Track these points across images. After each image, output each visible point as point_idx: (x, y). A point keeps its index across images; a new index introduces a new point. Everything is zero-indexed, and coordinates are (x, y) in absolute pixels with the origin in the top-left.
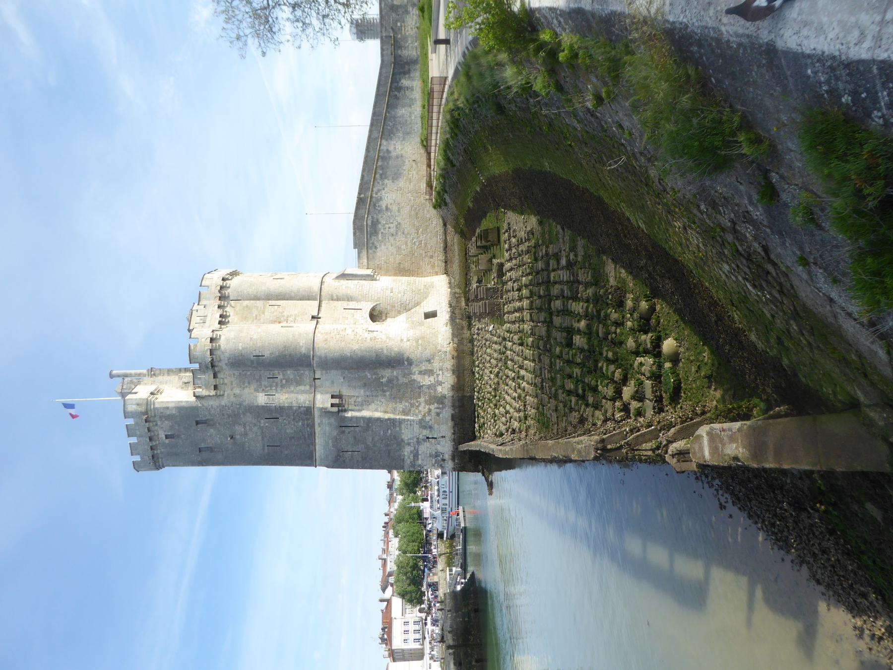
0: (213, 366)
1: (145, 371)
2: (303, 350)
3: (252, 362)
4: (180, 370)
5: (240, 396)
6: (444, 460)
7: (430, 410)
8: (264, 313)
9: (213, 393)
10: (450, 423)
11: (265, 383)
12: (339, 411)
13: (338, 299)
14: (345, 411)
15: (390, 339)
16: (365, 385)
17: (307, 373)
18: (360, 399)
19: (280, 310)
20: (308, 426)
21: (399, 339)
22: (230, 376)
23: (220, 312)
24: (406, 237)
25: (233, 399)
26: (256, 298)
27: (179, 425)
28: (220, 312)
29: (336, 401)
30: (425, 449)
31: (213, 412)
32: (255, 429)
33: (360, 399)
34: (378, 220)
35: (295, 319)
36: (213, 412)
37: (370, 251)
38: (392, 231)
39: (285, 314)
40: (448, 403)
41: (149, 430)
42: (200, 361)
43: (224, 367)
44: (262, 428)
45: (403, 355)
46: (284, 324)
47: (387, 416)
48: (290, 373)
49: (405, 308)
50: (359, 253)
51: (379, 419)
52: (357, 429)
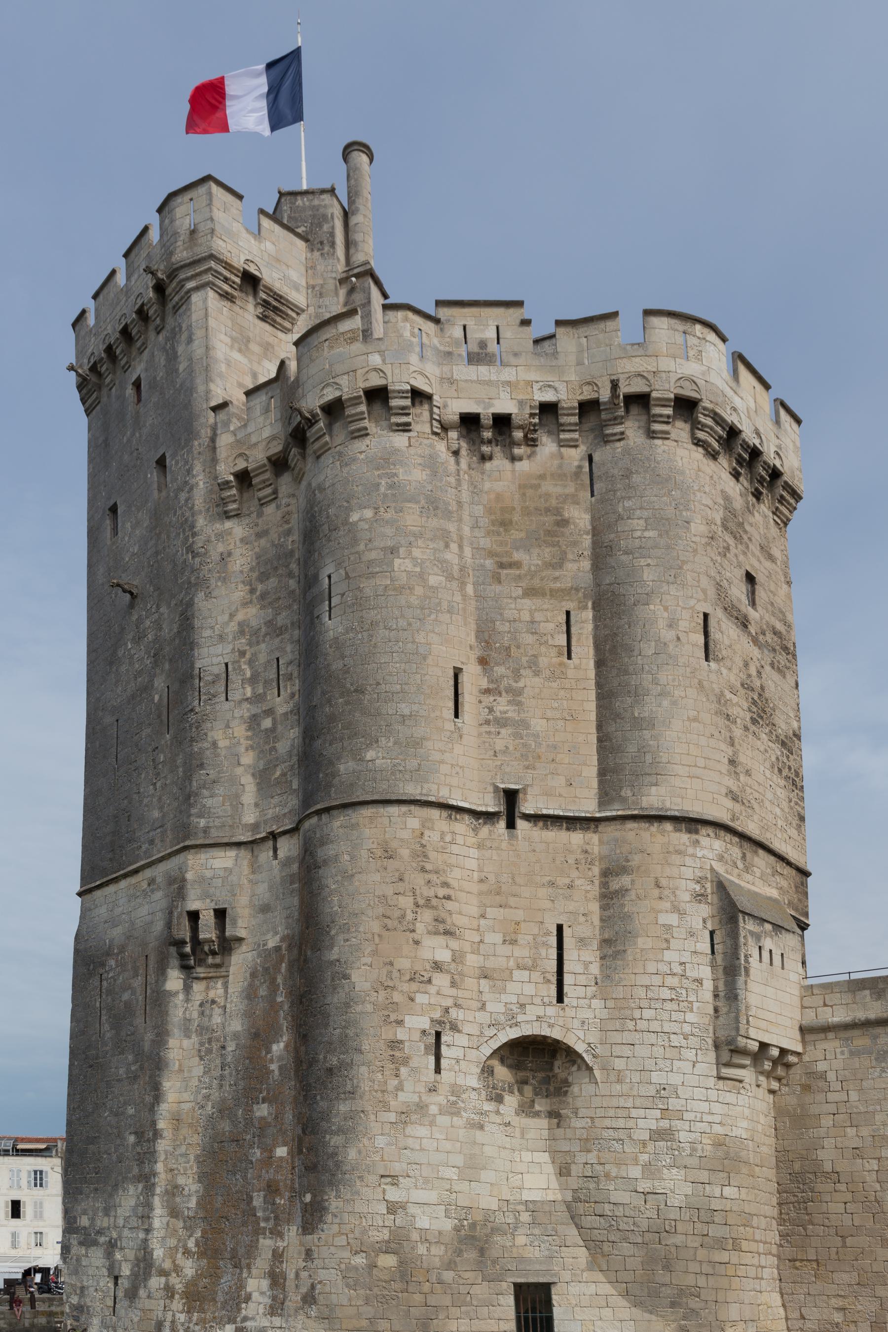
7: (170, 1292)
12: (181, 943)
29: (208, 931)
33: (217, 1019)
35: (502, 722)
39: (529, 682)
47: (161, 1125)
51: (157, 1096)
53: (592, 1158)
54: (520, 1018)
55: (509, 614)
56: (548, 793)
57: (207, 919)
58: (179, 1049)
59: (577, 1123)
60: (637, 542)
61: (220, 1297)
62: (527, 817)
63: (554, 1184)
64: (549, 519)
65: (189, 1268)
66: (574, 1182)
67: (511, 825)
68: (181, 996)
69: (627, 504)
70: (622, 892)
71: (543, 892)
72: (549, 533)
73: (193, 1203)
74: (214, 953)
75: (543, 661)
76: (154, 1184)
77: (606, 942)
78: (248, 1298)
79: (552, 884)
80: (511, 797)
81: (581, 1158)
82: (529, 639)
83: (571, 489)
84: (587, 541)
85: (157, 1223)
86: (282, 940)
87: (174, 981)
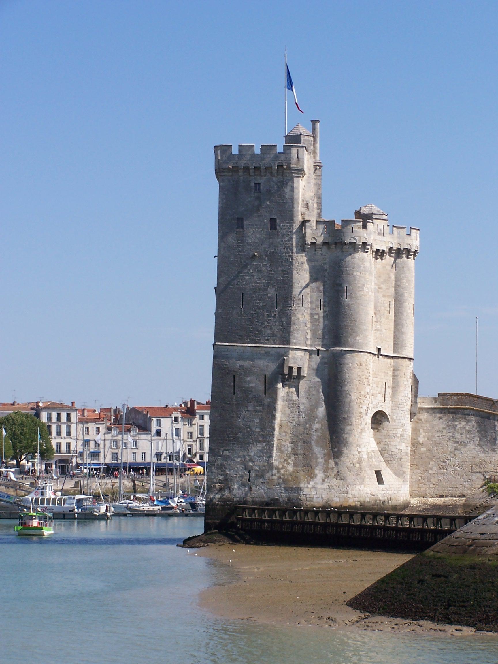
0: (336, 243)
1: (318, 159)
3: (341, 285)
4: (319, 197)
8: (384, 296)
9: (309, 240)
13: (394, 376)
14: (283, 382)
15: (361, 433)
18: (295, 397)
19: (386, 314)
20: (268, 340)
21: (361, 443)
23: (387, 250)
24: (451, 452)
26: (397, 286)
29: (295, 373)
31: (287, 238)
34: (469, 421)
35: (378, 330)
38: (458, 436)
39: (383, 320)
42: (344, 230)
45: (345, 446)
46: (374, 319)
49: (385, 452)
50: (435, 400)
51: (274, 417)
53: (387, 440)
55: (380, 301)
56: (385, 349)
59: (383, 431)
62: (382, 355)
63: (376, 446)
66: (382, 446)
67: (378, 357)
69: (403, 275)
70: (397, 376)
71: (383, 374)
73: (290, 449)
76: (273, 444)
77: (393, 387)
78: (317, 475)
79: (385, 372)
81: (384, 440)
82: (383, 308)
84: (394, 282)
85: (274, 455)
87: (280, 385)
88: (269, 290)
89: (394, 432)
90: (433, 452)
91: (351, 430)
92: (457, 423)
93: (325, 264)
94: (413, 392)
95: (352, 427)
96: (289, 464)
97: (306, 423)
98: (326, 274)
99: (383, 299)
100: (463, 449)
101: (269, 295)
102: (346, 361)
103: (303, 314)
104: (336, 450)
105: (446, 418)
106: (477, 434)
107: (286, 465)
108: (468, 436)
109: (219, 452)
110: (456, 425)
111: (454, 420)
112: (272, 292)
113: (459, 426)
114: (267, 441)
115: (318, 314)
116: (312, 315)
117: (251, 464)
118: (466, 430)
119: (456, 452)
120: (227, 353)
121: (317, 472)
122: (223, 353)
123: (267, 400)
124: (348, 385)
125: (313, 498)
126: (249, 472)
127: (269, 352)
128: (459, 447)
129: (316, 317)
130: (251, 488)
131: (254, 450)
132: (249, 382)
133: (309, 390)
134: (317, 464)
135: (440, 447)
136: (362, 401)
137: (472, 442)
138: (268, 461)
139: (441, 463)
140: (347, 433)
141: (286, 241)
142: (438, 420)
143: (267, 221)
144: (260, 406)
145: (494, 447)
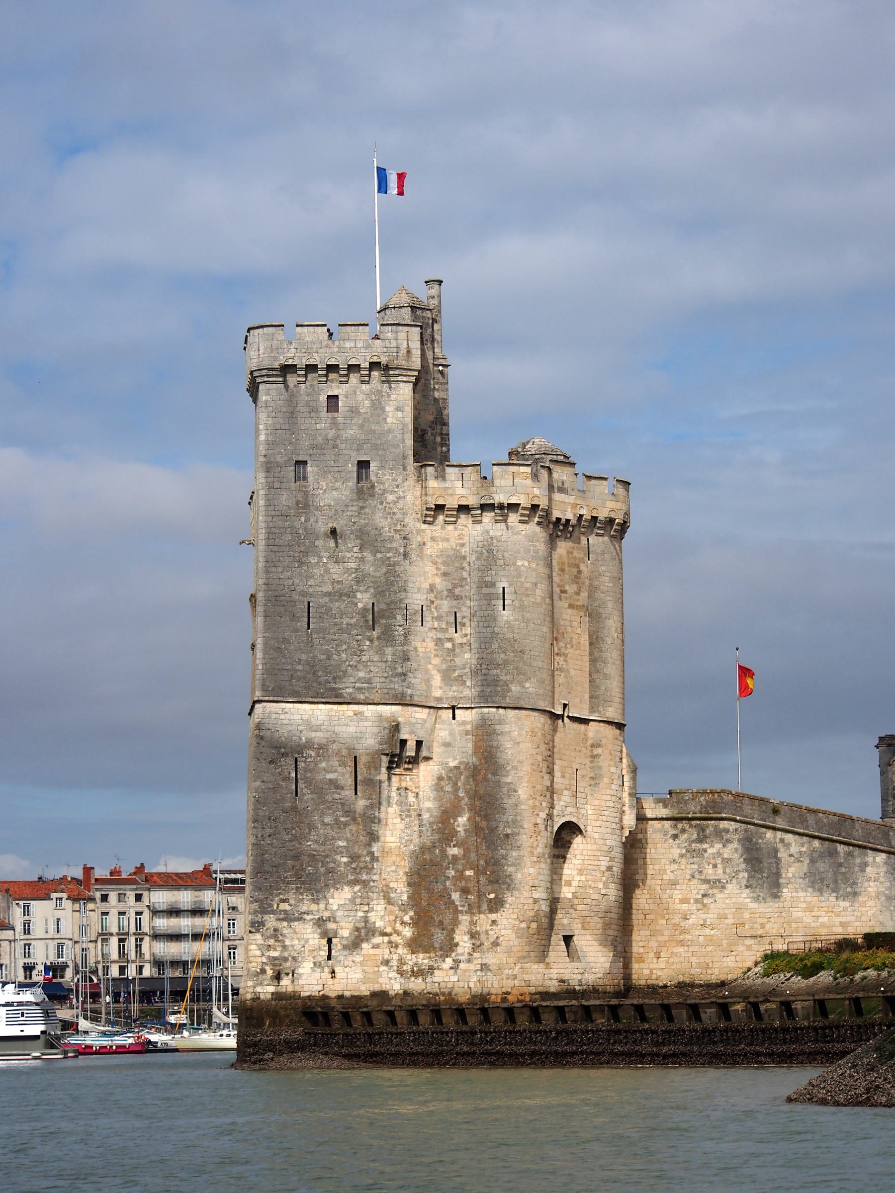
0: (484, 507)
2: (515, 688)
3: (493, 585)
5: (421, 556)
6: (278, 977)
8: (571, 606)
10: (365, 990)
11: (446, 605)
14: (389, 768)
16: (445, 812)
17: (467, 692)
18: (411, 798)
22: (461, 536)
24: (697, 901)
25: (416, 540)
27: (361, 426)
28: (574, 521)
29: (410, 751)
30: (305, 938)
31: (391, 498)
32: (348, 580)
33: (411, 798)
34: (729, 841)
36: (391, 498)
37: (667, 824)
38: (709, 871)
39: (569, 651)
40: (417, 985)
41: (354, 368)
43: (477, 527)
44: (350, 594)
48: (467, 657)
51: (373, 837)
52: (348, 793)
53: (583, 878)
54: (566, 813)
57: (411, 746)
58: (391, 814)
59: (574, 861)
60: (606, 589)
61: (437, 945)
64: (575, 570)
65: (408, 932)
66: (573, 889)
68: (386, 783)
69: (603, 568)
72: (576, 577)
73: (405, 897)
74: (409, 763)
75: (574, 642)
78: (457, 945)
80: (565, 706)
82: (569, 629)
83: (582, 556)
86: (461, 763)
87: (383, 775)
88: (359, 595)
89: (596, 863)
90: (664, 901)
91: (520, 858)
92: (705, 846)
93: (463, 545)
94: (626, 788)
95: (522, 853)
96: (402, 923)
97: (434, 847)
98: (465, 565)
99: (570, 611)
100: (719, 896)
101: (360, 605)
102: (506, 728)
103: (424, 641)
104: (492, 896)
105: (685, 836)
106: (743, 866)
107: (398, 926)
108: (728, 871)
109: (271, 906)
110: (705, 850)
111: (700, 840)
112: (364, 599)
113: (710, 851)
114: (364, 881)
115: (450, 640)
116: (439, 642)
117: (331, 926)
118: (723, 859)
119: (705, 901)
120: (282, 717)
121: (457, 938)
122: (274, 716)
123: (361, 804)
124: (513, 772)
125: (453, 988)
126: (329, 942)
127: (361, 713)
128: (710, 891)
129: (449, 645)
130: (333, 972)
131: (339, 898)
132: (326, 771)
133: (437, 784)
134: (456, 923)
135: (676, 892)
136: (537, 803)
137: (734, 881)
138: (366, 920)
139: (676, 921)
140: (511, 865)
141: (387, 503)
142: (671, 841)
143: (352, 468)
144: (348, 816)
145: (775, 891)
